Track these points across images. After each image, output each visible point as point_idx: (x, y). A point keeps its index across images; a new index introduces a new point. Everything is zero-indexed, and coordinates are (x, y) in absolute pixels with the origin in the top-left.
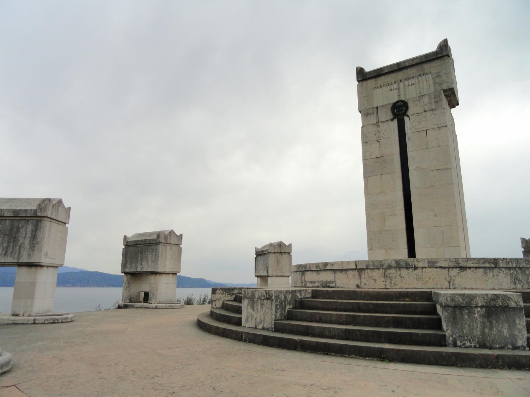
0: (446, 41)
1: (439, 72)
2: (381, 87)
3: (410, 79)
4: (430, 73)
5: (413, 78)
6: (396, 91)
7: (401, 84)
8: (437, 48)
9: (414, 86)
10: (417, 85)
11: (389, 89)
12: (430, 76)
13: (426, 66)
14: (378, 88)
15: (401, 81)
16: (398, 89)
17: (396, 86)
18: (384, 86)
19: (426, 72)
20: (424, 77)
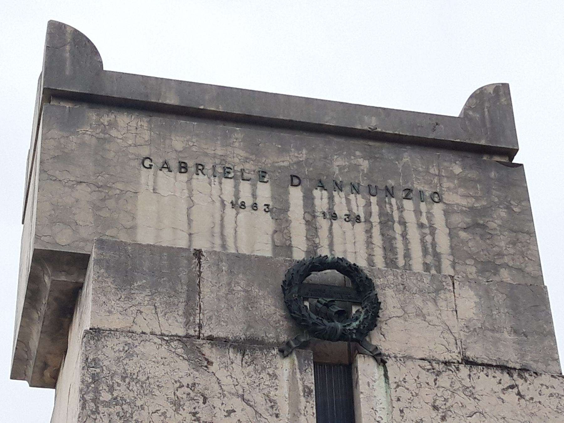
0: (501, 92)
1: (484, 212)
2: (183, 167)
3: (339, 187)
4: (436, 197)
5: (355, 188)
6: (266, 222)
7: (296, 195)
8: (468, 108)
9: (360, 228)
10: (376, 231)
11: (229, 197)
12: (438, 210)
13: (407, 157)
14: (166, 166)
15: (295, 180)
16: (279, 212)
17: (265, 192)
18: (200, 168)
19: (418, 186)
20: (408, 205)
